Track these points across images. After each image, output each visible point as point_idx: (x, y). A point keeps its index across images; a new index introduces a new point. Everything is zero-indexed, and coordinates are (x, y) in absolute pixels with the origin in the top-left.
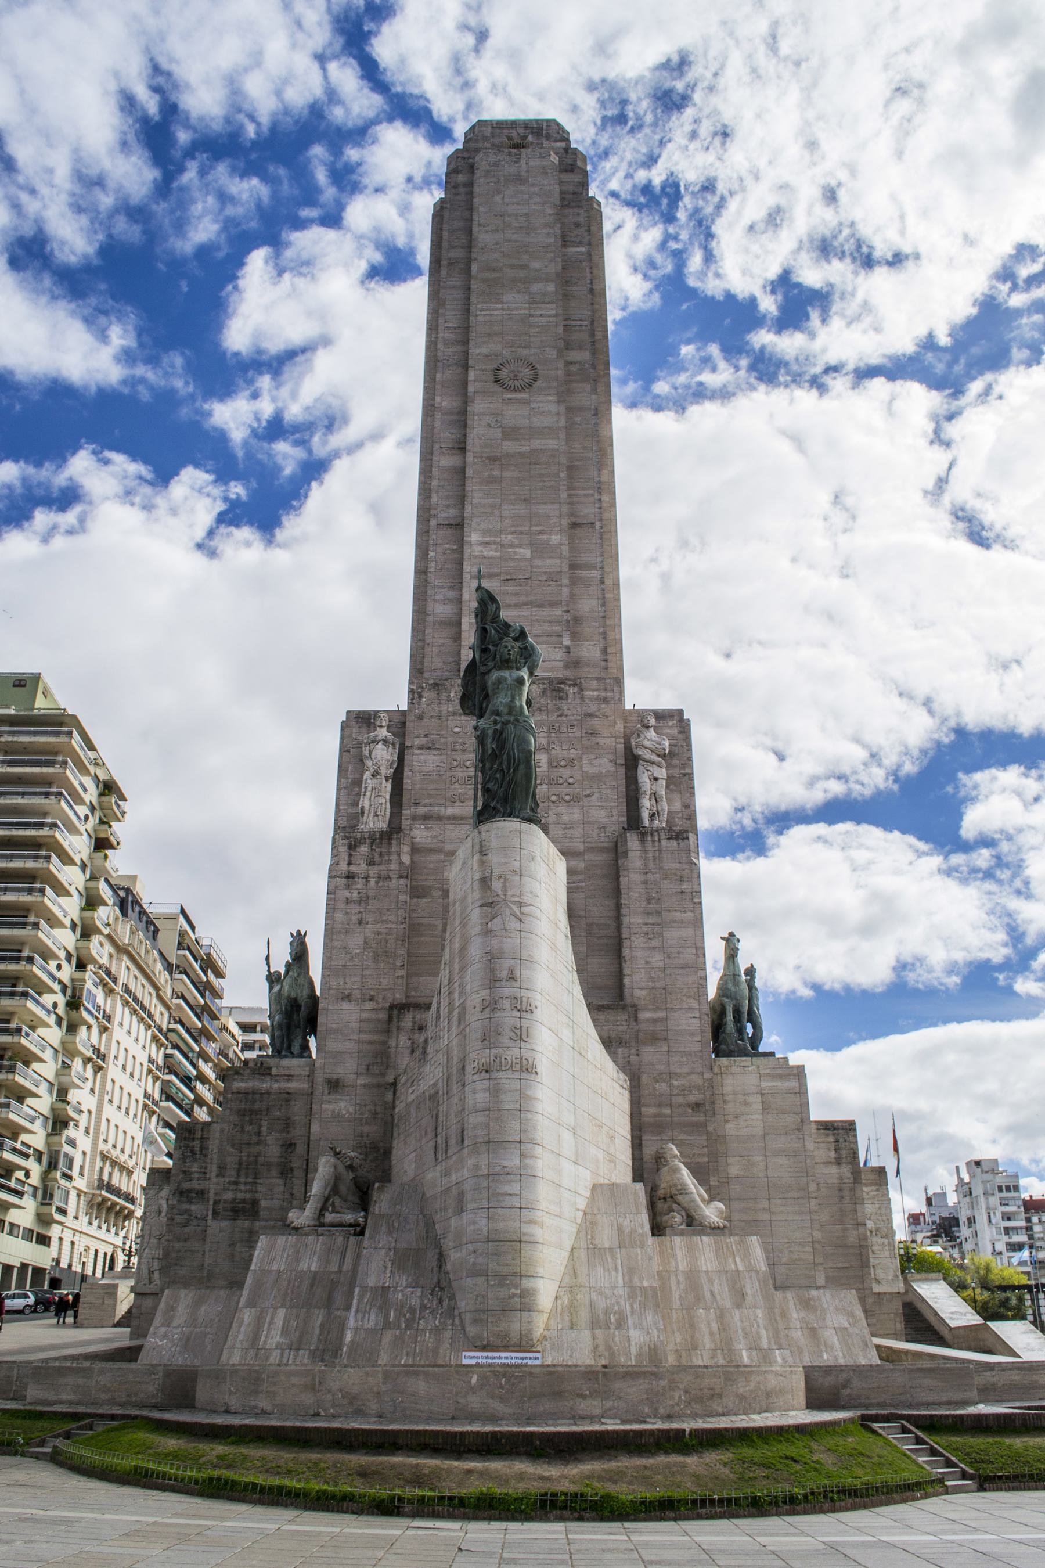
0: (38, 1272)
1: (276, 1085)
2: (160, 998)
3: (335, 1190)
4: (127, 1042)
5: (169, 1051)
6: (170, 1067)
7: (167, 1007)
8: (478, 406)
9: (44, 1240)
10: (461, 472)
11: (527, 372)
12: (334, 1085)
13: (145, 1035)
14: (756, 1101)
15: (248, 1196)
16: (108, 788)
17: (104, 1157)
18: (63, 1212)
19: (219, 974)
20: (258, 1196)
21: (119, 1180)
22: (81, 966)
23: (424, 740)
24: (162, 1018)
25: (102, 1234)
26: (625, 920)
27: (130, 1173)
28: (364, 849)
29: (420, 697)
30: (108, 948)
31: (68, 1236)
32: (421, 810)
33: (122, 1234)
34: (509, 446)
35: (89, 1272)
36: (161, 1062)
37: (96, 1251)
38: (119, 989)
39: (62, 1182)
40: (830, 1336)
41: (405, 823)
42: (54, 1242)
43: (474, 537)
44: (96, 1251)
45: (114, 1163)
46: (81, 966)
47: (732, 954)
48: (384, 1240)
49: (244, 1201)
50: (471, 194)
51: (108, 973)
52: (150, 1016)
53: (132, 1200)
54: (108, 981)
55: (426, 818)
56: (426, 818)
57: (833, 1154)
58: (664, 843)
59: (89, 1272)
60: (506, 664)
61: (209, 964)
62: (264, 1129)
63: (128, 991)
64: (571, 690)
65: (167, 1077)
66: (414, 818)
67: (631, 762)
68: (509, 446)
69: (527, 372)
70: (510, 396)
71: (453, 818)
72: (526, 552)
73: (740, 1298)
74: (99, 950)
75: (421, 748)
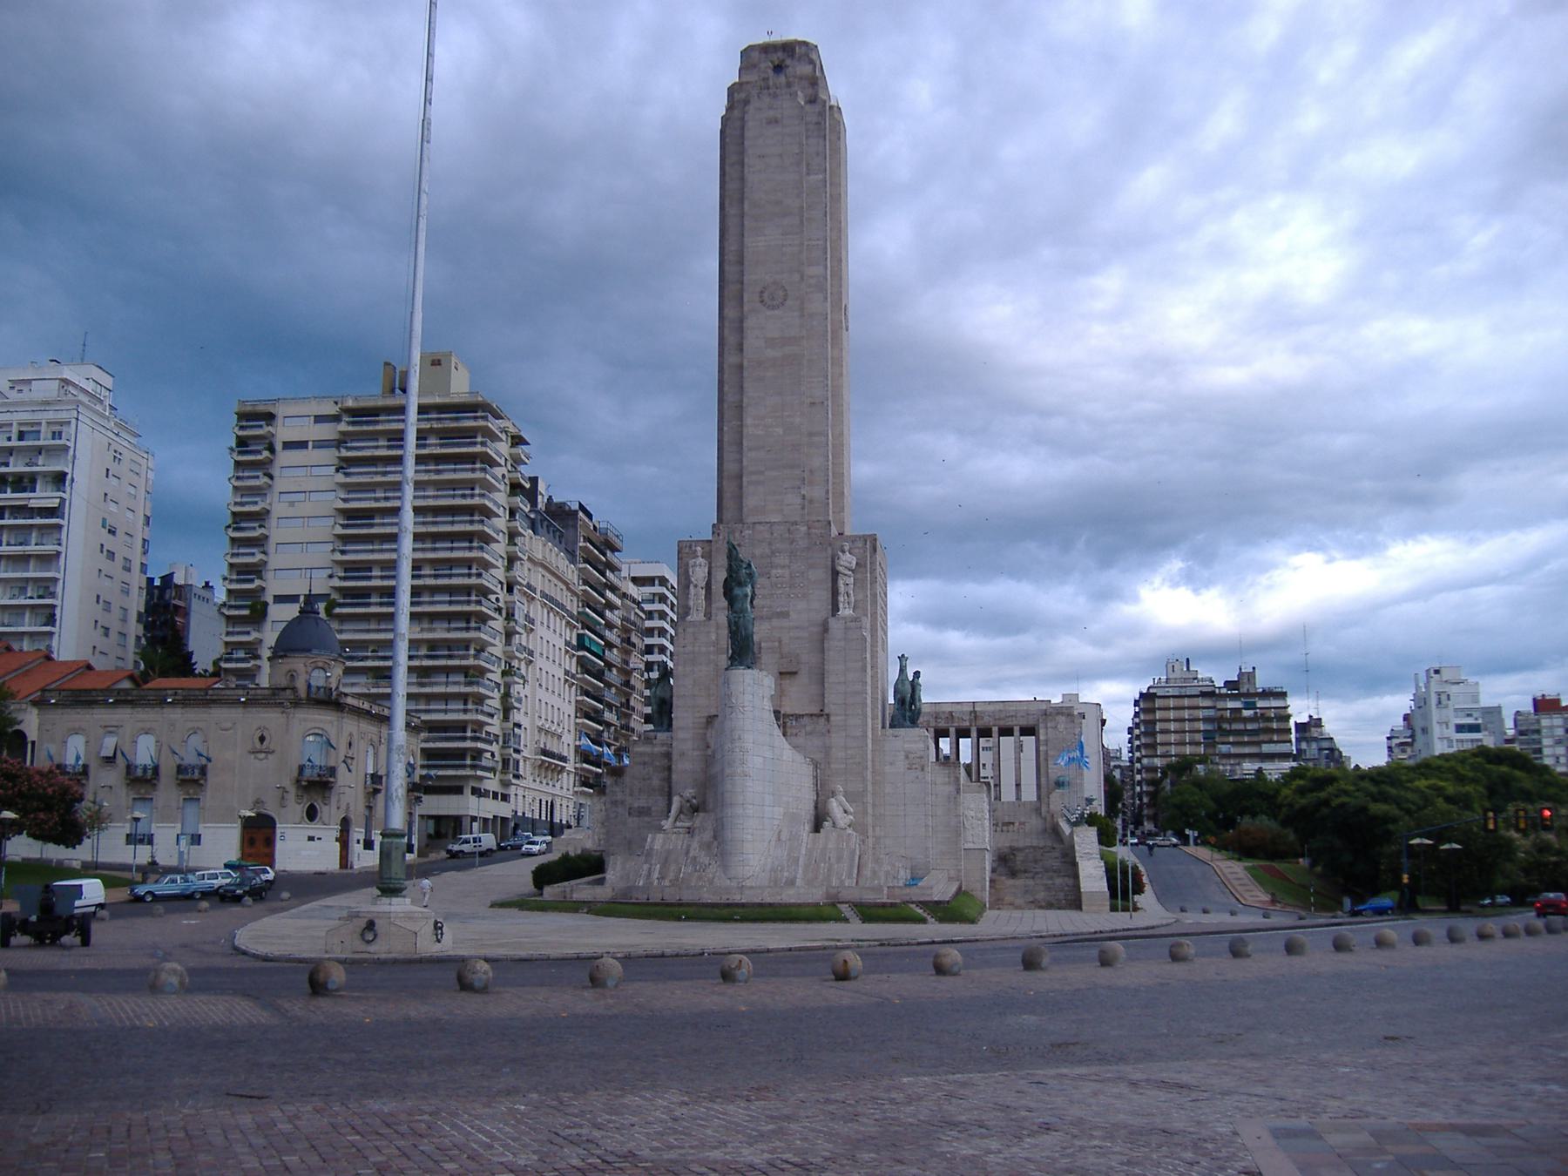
0: (504, 820)
2: (569, 589)
3: (681, 812)
4: (547, 635)
6: (581, 645)
7: (574, 593)
8: (750, 323)
9: (505, 798)
10: (741, 367)
11: (781, 293)
12: (682, 754)
13: (559, 625)
14: (902, 756)
16: (517, 441)
17: (540, 729)
18: (517, 777)
19: (614, 549)
21: (553, 746)
22: (510, 590)
24: (574, 606)
25: (543, 788)
27: (560, 737)
28: (690, 630)
30: (527, 565)
31: (520, 792)
33: (558, 785)
34: (770, 353)
36: (574, 642)
38: (538, 596)
39: (515, 756)
40: (882, 874)
42: (512, 798)
43: (748, 421)
45: (547, 732)
46: (510, 590)
47: (902, 670)
48: (697, 838)
50: (743, 128)
51: (529, 586)
52: (562, 607)
53: (564, 759)
54: (529, 593)
60: (740, 584)
61: (609, 546)
63: (544, 595)
65: (580, 653)
67: (835, 574)
68: (770, 353)
69: (781, 293)
70: (769, 313)
72: (780, 431)
73: (839, 859)
74: (522, 572)
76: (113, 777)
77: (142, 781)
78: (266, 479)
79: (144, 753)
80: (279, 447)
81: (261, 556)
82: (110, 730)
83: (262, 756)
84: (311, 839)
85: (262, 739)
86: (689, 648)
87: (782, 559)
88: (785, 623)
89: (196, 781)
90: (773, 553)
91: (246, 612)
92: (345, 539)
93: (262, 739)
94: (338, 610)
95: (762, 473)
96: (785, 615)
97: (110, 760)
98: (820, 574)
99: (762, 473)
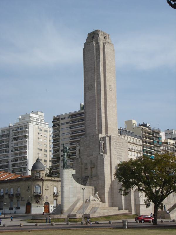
32: (82, 154)
64: (95, 137)
71: (85, 155)
72: (92, 116)
76: (6, 197)
77: (11, 197)
78: (58, 132)
79: (12, 191)
80: (60, 125)
81: (58, 148)
82: (6, 187)
83: (28, 191)
84: (37, 207)
85: (28, 187)
87: (91, 143)
88: (92, 157)
89: (11, 197)
90: (90, 142)
91: (56, 159)
92: (72, 142)
93: (28, 187)
94: (71, 157)
95: (89, 125)
96: (92, 155)
97: (7, 193)
98: (97, 146)
99: (89, 125)
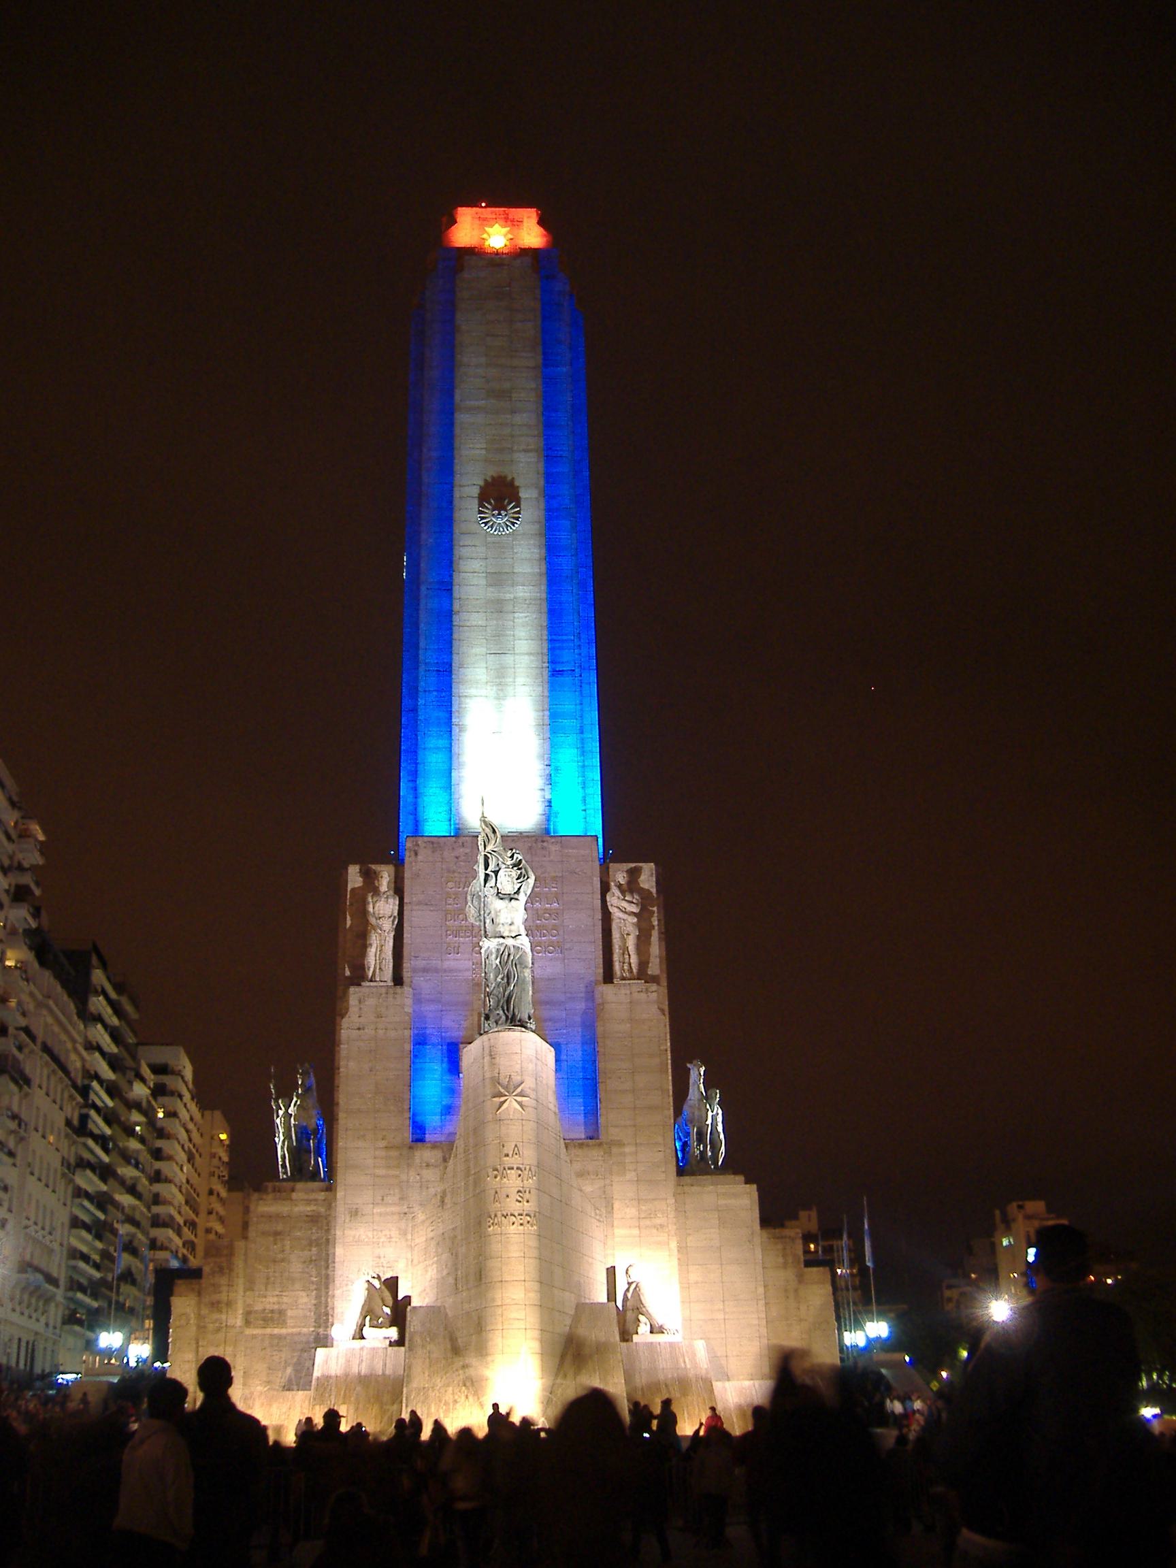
1: (296, 1209)
5: (85, 1111)
15: (276, 1307)
20: (284, 1307)
23: (421, 897)
26: (601, 1065)
28: (371, 1002)
29: (416, 854)
32: (420, 963)
35: (13, 1363)
37: (20, 1340)
41: (406, 975)
44: (20, 1340)
49: (272, 1311)
55: (425, 970)
56: (425, 970)
57: (781, 1260)
58: (636, 995)
59: (13, 1363)
62: (288, 1247)
66: (414, 970)
75: (419, 903)
86: (369, 1032)
